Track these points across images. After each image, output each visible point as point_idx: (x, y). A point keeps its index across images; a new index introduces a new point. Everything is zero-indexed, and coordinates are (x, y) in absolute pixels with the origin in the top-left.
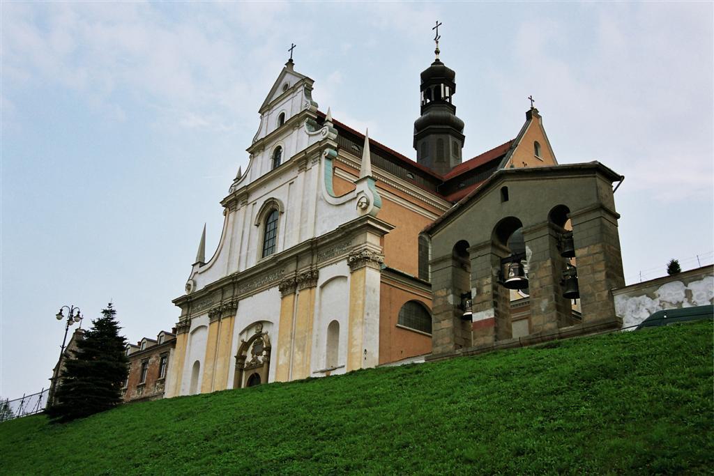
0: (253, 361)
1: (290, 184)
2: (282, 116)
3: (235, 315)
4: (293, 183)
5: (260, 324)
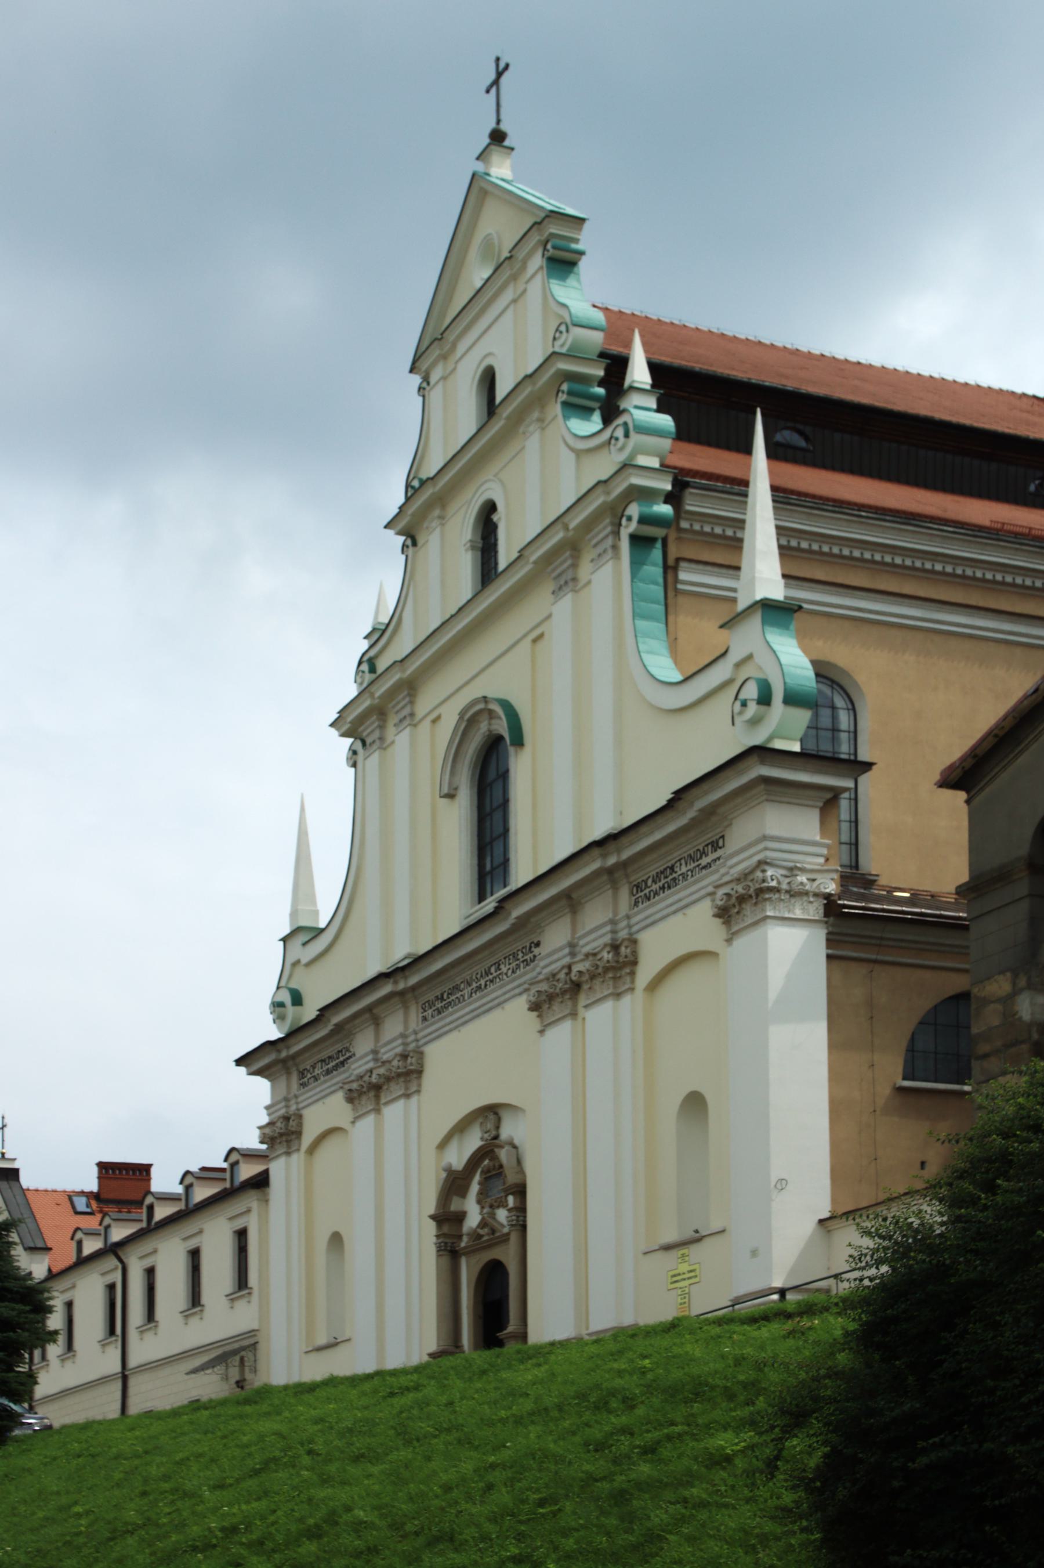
0: (483, 1224)
1: (535, 641)
2: (489, 379)
3: (418, 1091)
4: (541, 636)
5: (492, 1113)
